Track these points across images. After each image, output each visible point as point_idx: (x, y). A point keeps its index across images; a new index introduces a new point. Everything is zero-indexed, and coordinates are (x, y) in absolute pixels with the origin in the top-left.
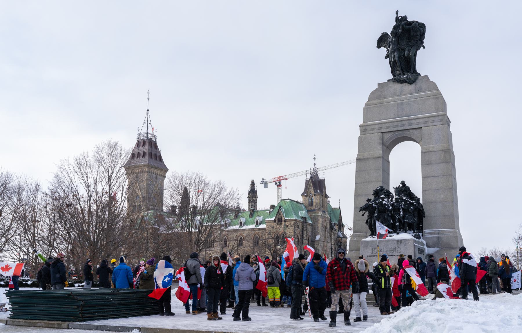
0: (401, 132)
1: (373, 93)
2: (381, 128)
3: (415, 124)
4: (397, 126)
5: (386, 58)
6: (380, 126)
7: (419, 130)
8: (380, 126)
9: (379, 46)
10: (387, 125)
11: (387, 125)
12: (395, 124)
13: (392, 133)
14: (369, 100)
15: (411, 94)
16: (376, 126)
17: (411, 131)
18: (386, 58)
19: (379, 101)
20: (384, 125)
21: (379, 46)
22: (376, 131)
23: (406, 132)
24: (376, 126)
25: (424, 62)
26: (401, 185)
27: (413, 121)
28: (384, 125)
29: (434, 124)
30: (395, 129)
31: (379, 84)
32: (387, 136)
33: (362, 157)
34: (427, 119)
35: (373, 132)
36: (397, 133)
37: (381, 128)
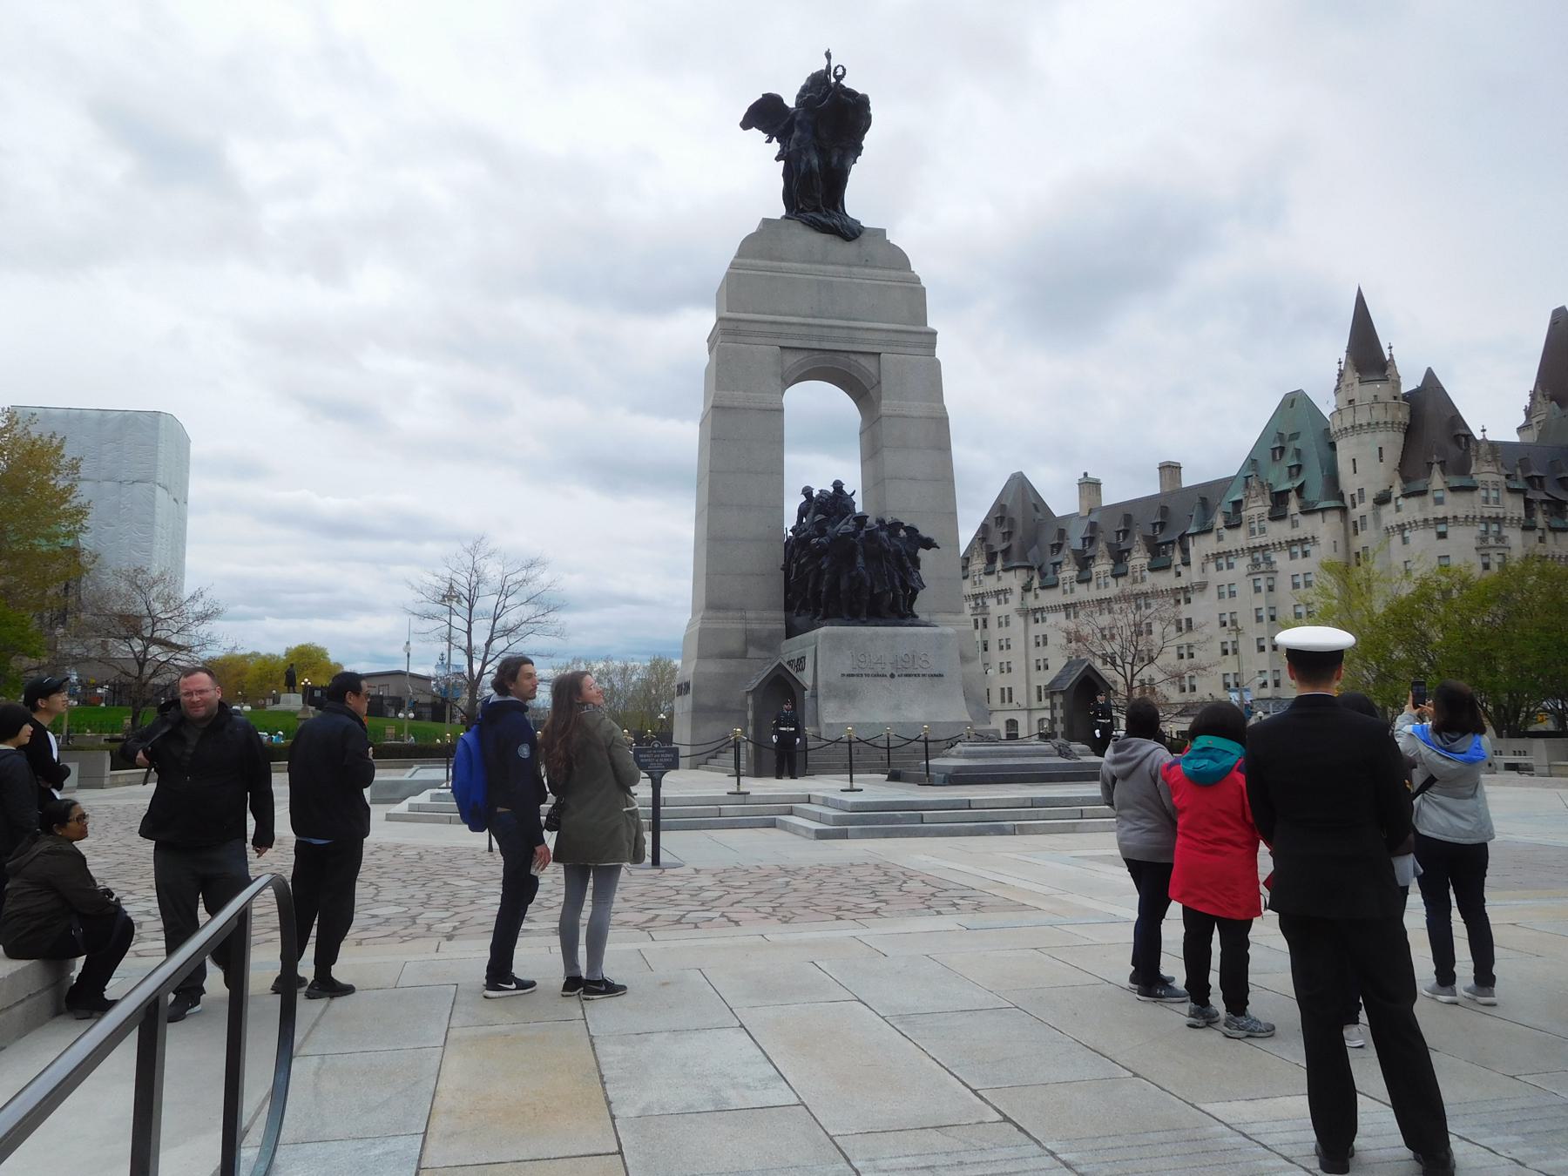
0: (828, 355)
1: (749, 240)
2: (779, 335)
3: (852, 341)
4: (821, 338)
5: (778, 159)
6: (775, 328)
7: (873, 359)
8: (775, 328)
9: (746, 124)
10: (794, 330)
11: (794, 330)
12: (815, 331)
13: (806, 353)
14: (740, 254)
15: (849, 265)
16: (766, 328)
17: (853, 357)
18: (778, 159)
19: (769, 263)
20: (786, 329)
21: (746, 124)
22: (763, 340)
23: (841, 357)
24: (766, 328)
25: (864, 194)
26: (831, 490)
27: (858, 334)
28: (786, 329)
29: (909, 350)
30: (815, 345)
31: (766, 222)
32: (791, 359)
33: (727, 403)
34: (894, 337)
35: (757, 340)
36: (816, 355)
37: (779, 335)
